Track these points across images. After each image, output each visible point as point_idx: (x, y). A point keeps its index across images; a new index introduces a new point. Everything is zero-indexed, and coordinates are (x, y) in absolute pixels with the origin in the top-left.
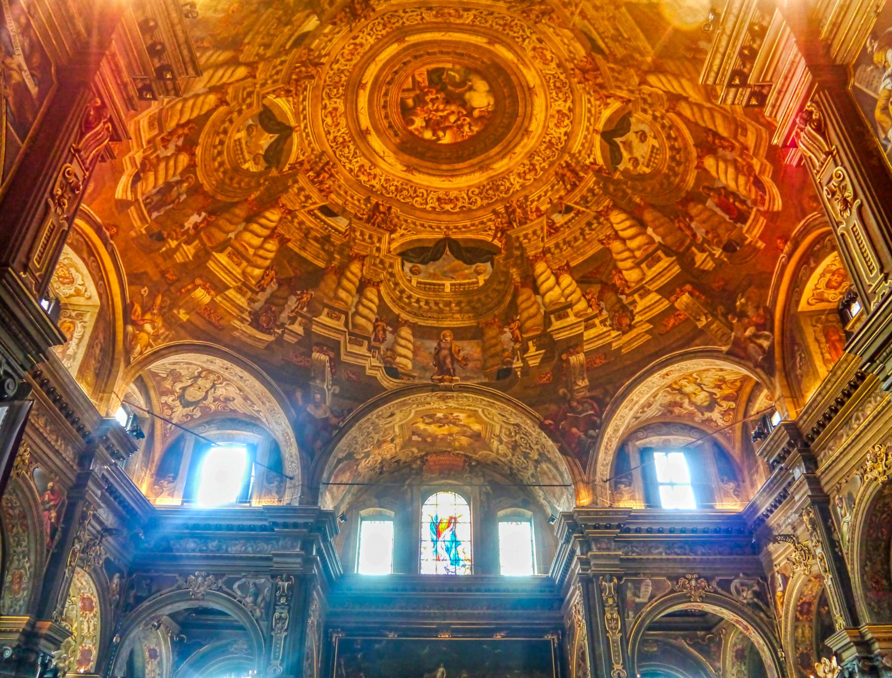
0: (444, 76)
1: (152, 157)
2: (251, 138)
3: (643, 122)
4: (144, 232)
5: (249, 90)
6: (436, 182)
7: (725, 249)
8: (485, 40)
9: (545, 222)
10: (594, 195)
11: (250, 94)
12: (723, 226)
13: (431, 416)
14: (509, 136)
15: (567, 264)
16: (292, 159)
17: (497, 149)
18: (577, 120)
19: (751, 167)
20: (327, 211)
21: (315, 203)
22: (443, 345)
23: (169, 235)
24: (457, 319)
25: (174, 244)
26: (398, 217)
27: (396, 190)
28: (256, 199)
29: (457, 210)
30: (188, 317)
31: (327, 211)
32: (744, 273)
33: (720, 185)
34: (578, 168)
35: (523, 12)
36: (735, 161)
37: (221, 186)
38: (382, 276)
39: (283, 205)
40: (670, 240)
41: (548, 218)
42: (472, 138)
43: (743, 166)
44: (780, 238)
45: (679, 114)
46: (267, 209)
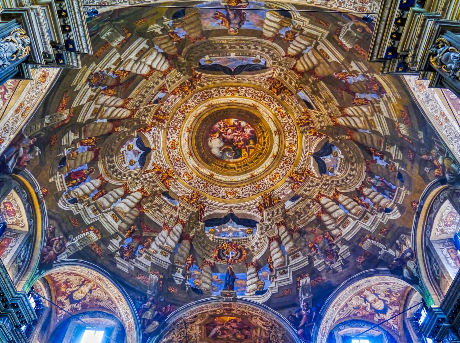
0: (234, 154)
1: (376, 209)
2: (333, 167)
3: (134, 169)
4: (404, 187)
5: (324, 187)
6: (240, 100)
7: (64, 158)
8: (215, 177)
9: (169, 90)
10: (144, 115)
11: (325, 184)
12: (73, 166)
14: (198, 124)
15: (147, 79)
16: (319, 140)
17: (204, 117)
18: (165, 149)
19: (82, 202)
20: (309, 105)
21: (315, 112)
22: (237, 26)
23: (396, 171)
25: (397, 164)
26: (265, 84)
27: (264, 98)
28: (346, 135)
29: (226, 87)
30: (419, 132)
31: (309, 105)
32: (47, 163)
33: (87, 180)
34: (157, 123)
35: (200, 195)
36: (89, 196)
37: (358, 161)
39: (333, 121)
40: (92, 126)
41: (167, 93)
42: (219, 121)
43: (84, 198)
44: (47, 193)
45: (120, 186)
46: (342, 126)
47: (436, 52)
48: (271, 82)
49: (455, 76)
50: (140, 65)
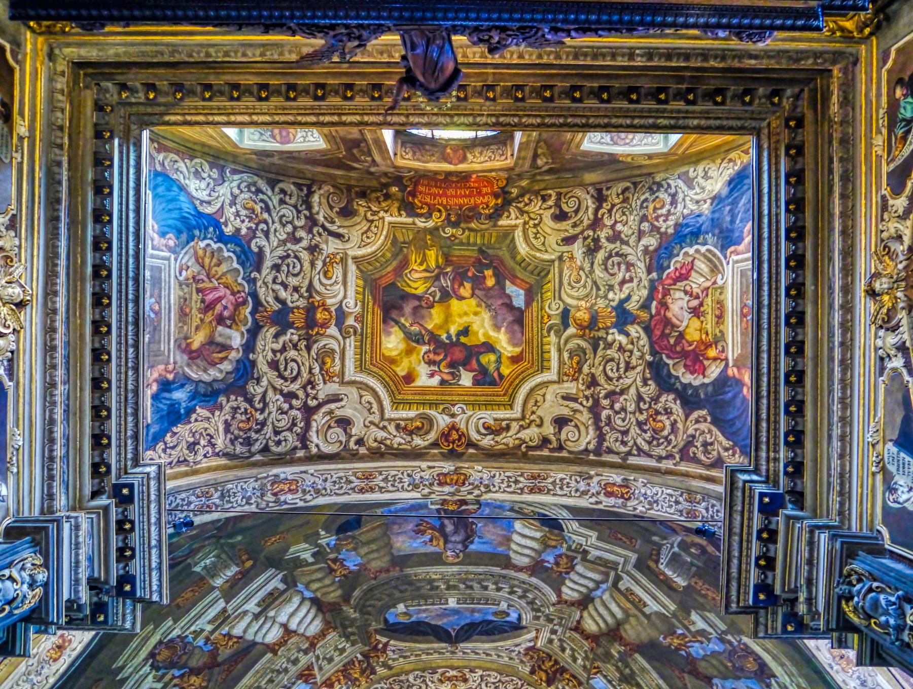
9: (318, 677)
13: (483, 378)
15: (275, 653)
22: (460, 546)
24: (436, 573)
26: (522, 662)
38: (551, 609)
41: (315, 683)
47: (850, 592)
48: (532, 658)
49: (902, 641)
50: (264, 623)
